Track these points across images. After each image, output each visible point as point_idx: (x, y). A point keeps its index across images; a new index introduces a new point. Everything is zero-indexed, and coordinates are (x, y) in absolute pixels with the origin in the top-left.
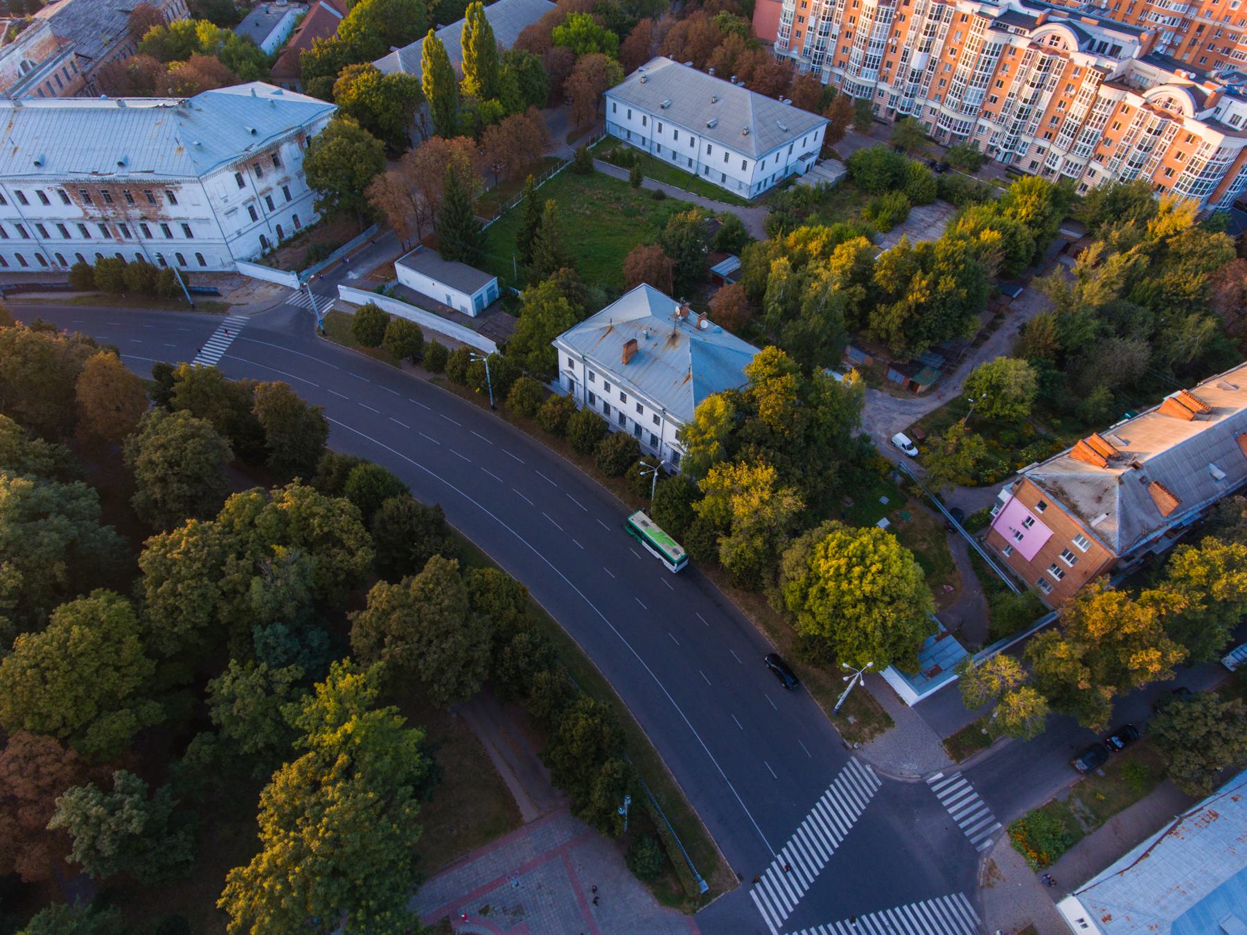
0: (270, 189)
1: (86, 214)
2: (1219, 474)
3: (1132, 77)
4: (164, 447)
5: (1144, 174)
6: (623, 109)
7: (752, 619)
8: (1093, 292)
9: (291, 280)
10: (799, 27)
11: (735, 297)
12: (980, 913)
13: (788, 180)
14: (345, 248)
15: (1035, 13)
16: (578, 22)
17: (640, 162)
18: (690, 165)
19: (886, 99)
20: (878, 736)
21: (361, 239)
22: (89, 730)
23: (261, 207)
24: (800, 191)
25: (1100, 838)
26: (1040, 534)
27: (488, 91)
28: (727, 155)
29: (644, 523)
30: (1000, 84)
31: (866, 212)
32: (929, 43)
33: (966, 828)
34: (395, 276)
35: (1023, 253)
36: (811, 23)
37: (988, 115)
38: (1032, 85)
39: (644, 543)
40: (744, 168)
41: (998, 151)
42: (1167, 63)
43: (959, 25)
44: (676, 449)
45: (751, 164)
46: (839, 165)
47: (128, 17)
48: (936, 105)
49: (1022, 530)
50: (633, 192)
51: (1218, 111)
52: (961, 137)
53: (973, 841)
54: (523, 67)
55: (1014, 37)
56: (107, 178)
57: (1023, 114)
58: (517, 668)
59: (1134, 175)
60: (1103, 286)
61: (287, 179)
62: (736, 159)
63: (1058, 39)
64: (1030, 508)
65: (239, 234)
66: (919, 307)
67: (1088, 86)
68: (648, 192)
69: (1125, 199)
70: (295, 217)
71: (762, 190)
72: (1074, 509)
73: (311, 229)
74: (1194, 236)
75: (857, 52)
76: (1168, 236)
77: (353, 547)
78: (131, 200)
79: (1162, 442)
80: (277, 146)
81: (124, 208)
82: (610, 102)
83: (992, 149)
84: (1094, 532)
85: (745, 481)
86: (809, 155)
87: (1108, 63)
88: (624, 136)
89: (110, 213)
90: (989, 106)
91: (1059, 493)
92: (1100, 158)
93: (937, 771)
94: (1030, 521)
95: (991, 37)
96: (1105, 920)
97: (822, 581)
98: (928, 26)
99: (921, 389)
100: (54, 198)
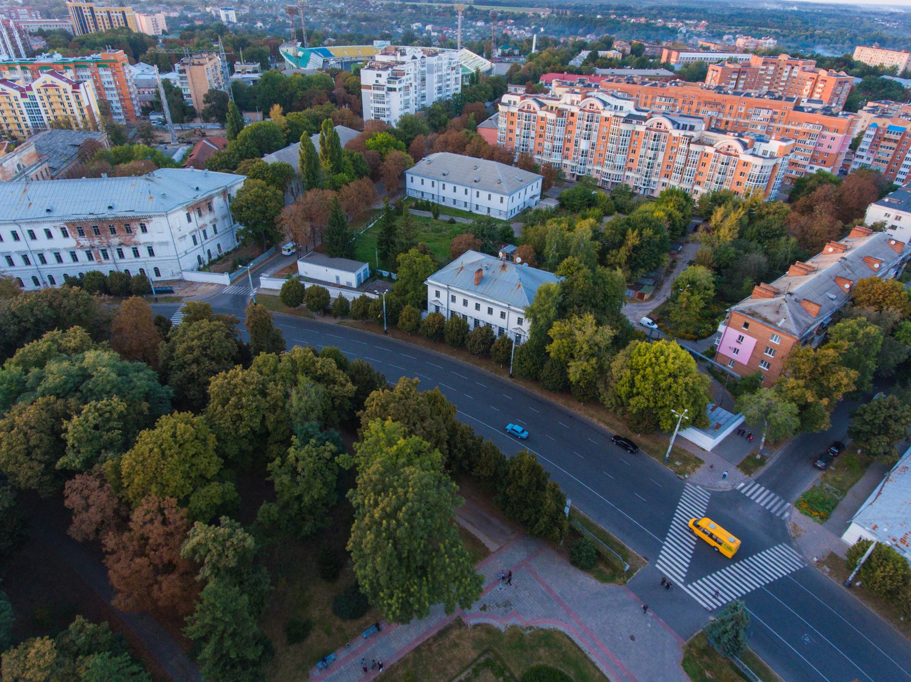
0: (205, 225)
1: (78, 243)
2: (833, 296)
4: (199, 338)
5: (725, 187)
6: (417, 180)
7: (595, 420)
9: (224, 279)
10: (511, 135)
12: (800, 552)
14: (256, 260)
15: (645, 114)
16: (381, 137)
17: (433, 208)
18: (466, 206)
19: (569, 168)
20: (697, 470)
21: (265, 255)
22: (192, 498)
23: (200, 236)
25: (848, 500)
26: (750, 342)
27: (337, 169)
28: (490, 196)
32: (589, 135)
33: (771, 509)
34: (297, 270)
35: (678, 224)
36: (518, 132)
37: (630, 169)
40: (502, 201)
41: (640, 189)
44: (517, 332)
45: (506, 198)
47: (77, 148)
48: (599, 168)
49: (737, 346)
50: (435, 221)
51: (754, 150)
53: (778, 514)
54: (354, 158)
56: (100, 216)
57: (650, 166)
58: (466, 447)
60: (730, 230)
61: (215, 220)
62: (496, 197)
65: (186, 253)
66: (635, 249)
67: (683, 146)
68: (445, 221)
70: (219, 245)
71: (513, 215)
73: (228, 254)
75: (547, 145)
76: (753, 206)
77: (344, 382)
78: (113, 231)
80: (211, 197)
81: (108, 238)
82: (408, 177)
84: (780, 330)
86: (534, 196)
87: (689, 133)
88: (419, 196)
89: (96, 242)
90: (630, 165)
91: (753, 314)
92: (699, 183)
93: (740, 482)
94: (741, 338)
96: (874, 529)
97: (642, 372)
99: (646, 297)
100: (57, 233)
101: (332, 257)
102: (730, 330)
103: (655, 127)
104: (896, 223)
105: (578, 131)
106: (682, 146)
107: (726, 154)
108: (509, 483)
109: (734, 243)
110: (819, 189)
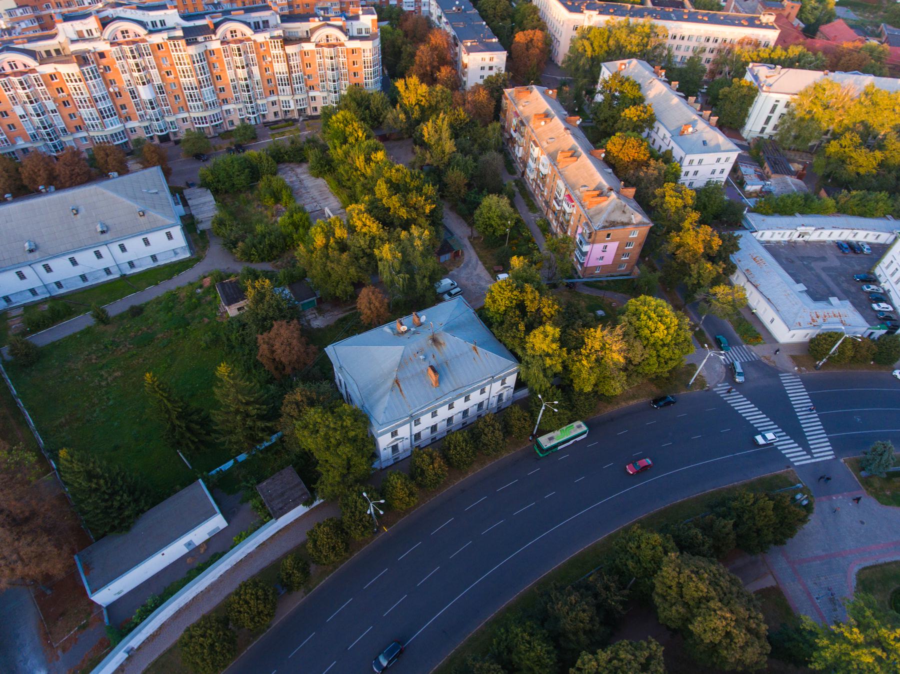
3: (287, 35)
8: (449, 146)
11: (380, 296)
13: (189, 224)
24: (220, 223)
26: (613, 247)
29: (551, 439)
30: (219, 78)
31: (270, 202)
37: (225, 101)
38: (243, 67)
39: (559, 448)
41: (249, 119)
42: (305, 18)
43: (159, 53)
46: (197, 191)
48: (186, 115)
50: (110, 329)
52: (217, 126)
55: (207, 44)
59: (340, 84)
62: (158, 239)
64: (605, 241)
66: (432, 211)
67: (278, 51)
68: (121, 316)
69: (362, 100)
74: (430, 94)
75: (85, 112)
79: (592, 175)
83: (243, 120)
85: (597, 346)
90: (223, 95)
91: (613, 224)
92: (312, 88)
95: (193, 50)
98: (137, 65)
101: (128, 528)
102: (596, 246)
103: (229, 36)
104: (492, 64)
105: (126, 77)
106: (274, 52)
107: (330, 46)
108: (758, 531)
109: (462, 149)
110: (418, 53)
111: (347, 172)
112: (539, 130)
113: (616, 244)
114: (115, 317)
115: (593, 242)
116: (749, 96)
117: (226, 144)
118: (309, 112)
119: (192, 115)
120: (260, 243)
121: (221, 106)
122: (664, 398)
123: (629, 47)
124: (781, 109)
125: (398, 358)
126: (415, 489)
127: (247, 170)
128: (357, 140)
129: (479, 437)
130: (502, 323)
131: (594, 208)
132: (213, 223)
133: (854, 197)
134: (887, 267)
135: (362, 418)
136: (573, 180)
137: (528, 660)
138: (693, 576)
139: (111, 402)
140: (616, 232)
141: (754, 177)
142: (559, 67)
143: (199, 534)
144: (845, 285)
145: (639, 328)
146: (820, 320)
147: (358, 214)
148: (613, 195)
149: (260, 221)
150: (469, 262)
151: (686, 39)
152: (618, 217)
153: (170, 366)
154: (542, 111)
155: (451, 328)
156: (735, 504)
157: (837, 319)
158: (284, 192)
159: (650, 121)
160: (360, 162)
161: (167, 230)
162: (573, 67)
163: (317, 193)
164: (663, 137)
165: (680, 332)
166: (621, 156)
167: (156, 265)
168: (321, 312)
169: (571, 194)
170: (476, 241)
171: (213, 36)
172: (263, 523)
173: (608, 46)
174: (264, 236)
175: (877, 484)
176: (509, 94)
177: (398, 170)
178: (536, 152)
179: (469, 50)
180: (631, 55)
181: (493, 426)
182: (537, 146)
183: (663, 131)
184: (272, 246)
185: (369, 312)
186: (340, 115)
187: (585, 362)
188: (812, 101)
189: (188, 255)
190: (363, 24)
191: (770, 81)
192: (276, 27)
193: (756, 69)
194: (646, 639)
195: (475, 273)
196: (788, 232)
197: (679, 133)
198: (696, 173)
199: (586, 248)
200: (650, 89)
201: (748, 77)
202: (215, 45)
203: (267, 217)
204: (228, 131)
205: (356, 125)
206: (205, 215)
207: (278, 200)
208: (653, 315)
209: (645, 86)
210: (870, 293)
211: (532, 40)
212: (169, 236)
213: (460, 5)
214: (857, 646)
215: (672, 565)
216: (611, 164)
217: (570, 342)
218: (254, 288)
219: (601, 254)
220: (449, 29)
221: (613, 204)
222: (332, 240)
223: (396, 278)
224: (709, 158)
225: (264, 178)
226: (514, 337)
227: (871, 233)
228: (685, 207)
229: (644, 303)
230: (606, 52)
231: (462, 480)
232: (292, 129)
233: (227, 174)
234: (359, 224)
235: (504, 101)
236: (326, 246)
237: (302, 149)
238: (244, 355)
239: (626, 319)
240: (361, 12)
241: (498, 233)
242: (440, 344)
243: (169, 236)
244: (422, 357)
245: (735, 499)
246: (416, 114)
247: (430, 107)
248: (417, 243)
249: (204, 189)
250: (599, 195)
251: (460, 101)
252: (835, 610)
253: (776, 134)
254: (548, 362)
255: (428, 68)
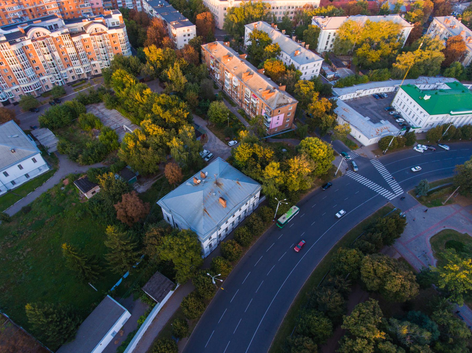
3: (71, 31)
8: (183, 80)
12: (373, 159)
26: (282, 116)
29: (284, 218)
37: (41, 75)
38: (48, 53)
41: (58, 83)
42: (79, 20)
52: (38, 90)
55: (23, 42)
59: (108, 55)
63: (39, 33)
64: (278, 114)
67: (68, 41)
68: (18, 215)
72: (286, 104)
79: (262, 83)
83: (54, 84)
90: (38, 72)
91: (280, 105)
92: (92, 59)
95: (14, 47)
101: (74, 337)
103: (35, 36)
104: (189, 33)
111: (131, 103)
112: (227, 64)
113: (283, 115)
114: (13, 216)
115: (273, 116)
116: (317, 32)
117: (48, 99)
118: (93, 73)
119: (22, 86)
120: (92, 153)
121: (39, 78)
122: (326, 184)
123: (255, 16)
124: (332, 37)
125: (202, 198)
126: (230, 263)
127: (69, 113)
128: (131, 85)
129: (252, 227)
130: (246, 167)
131: (269, 99)
132: (58, 147)
133: (375, 73)
134: (397, 102)
135: (193, 234)
136: (254, 87)
137: (320, 329)
138: (379, 264)
139: (31, 268)
140: (282, 109)
141: (329, 71)
142: (221, 30)
143: (117, 327)
144: (382, 114)
145: (311, 153)
146: (380, 132)
147: (148, 125)
148: (277, 91)
149: (86, 141)
150: (211, 139)
151: (279, 8)
152: (282, 101)
153: (61, 236)
154: (226, 54)
155: (223, 175)
156: (378, 225)
157: (386, 130)
158: (96, 121)
159: (278, 51)
160: (137, 96)
161: (33, 157)
162: (230, 29)
163: (115, 118)
164: (286, 58)
165: (329, 151)
166: (273, 71)
167: (29, 179)
168: (141, 183)
169: (255, 94)
170: (211, 127)
171: (26, 38)
172: (152, 307)
173: (245, 16)
174: (93, 148)
175: (424, 199)
176: (205, 47)
177: (163, 97)
178: (229, 75)
179: (176, 27)
180: (257, 20)
181: (257, 219)
182: (229, 72)
183: (285, 55)
184: (100, 153)
185: (173, 177)
186: (118, 72)
187: (293, 176)
188: (345, 31)
189: (48, 169)
190: (115, 20)
191: (325, 24)
192: (63, 27)
193: (316, 19)
194: (369, 300)
195: (216, 144)
196: (353, 94)
197: (294, 55)
198: (306, 73)
199: (269, 120)
200: (273, 36)
201: (314, 23)
202: (28, 42)
203: (89, 137)
204: (46, 92)
205: (128, 76)
206: (51, 144)
207: (93, 126)
208: (316, 146)
209: (270, 33)
210: (393, 115)
211: (206, 18)
212: (34, 161)
213: (162, 3)
214: (457, 272)
215: (369, 262)
216: (268, 75)
217: (285, 168)
218: (104, 179)
219: (277, 121)
220: (159, 16)
221: (278, 95)
222: (138, 142)
223: (182, 155)
224: (310, 65)
225: (81, 115)
226: (256, 172)
227: (386, 88)
228: (311, 91)
229: (309, 141)
230: (244, 19)
231: (247, 251)
232: (86, 84)
233: (57, 117)
234: (151, 131)
235: (203, 52)
236: (135, 147)
237: (97, 95)
238: (105, 218)
239: (304, 150)
240: (112, 13)
241: (223, 120)
242: (221, 185)
243: (34, 161)
244: (214, 194)
245: (377, 223)
246: (159, 65)
247: (165, 60)
248: (189, 134)
249: (44, 129)
250: (269, 92)
251: (180, 55)
252: (427, 260)
253: (333, 49)
254: (277, 180)
255: (156, 40)
